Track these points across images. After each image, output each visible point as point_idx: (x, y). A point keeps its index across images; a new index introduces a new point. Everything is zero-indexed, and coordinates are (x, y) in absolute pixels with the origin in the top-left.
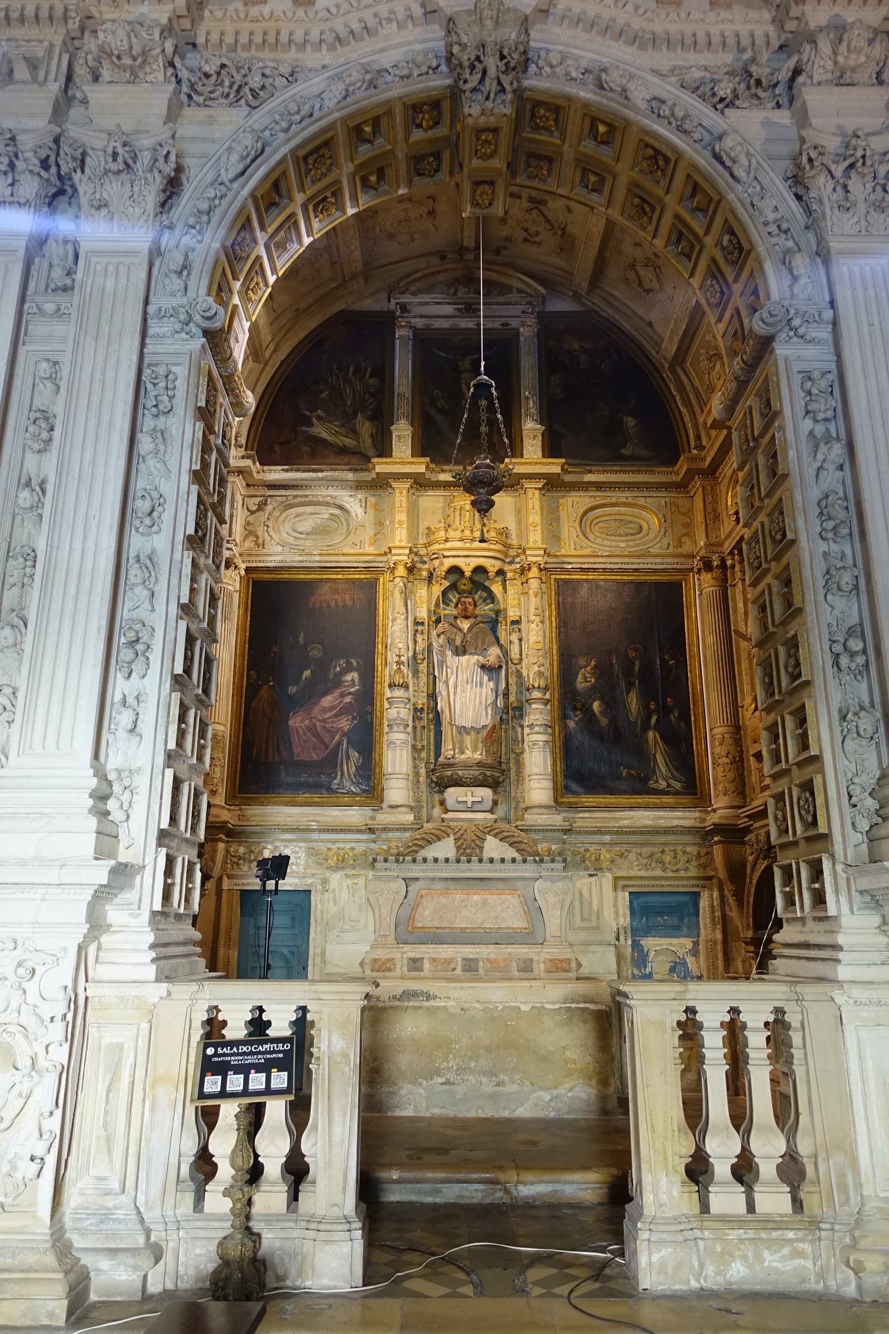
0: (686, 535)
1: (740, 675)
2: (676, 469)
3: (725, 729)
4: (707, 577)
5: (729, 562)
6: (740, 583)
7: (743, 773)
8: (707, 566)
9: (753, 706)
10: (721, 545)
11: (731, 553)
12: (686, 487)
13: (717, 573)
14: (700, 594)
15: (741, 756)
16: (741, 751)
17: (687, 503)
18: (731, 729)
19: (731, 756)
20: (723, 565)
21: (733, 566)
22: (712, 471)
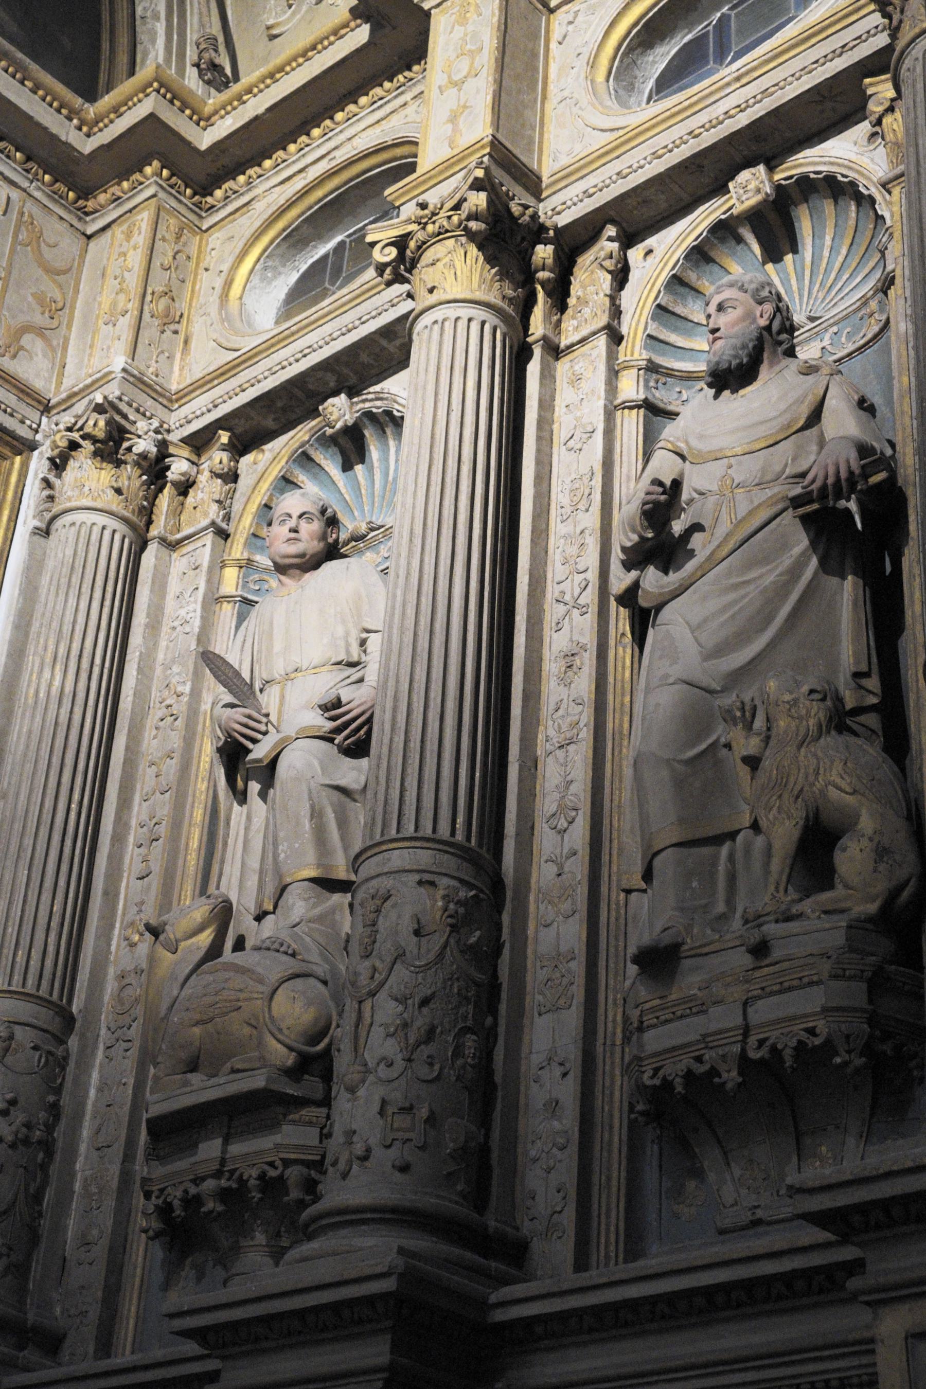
0: (40, 332)
1: (119, 839)
2: (91, 111)
3: (24, 1010)
4: (88, 478)
5: (178, 467)
6: (206, 546)
7: (38, 1198)
8: (111, 446)
9: (206, 938)
10: (171, 400)
11: (199, 442)
12: (85, 193)
13: (131, 478)
14: (45, 532)
15: (50, 1128)
16: (55, 1110)
17: (69, 244)
18: (44, 1016)
19: (19, 1117)
20: (155, 469)
21: (185, 487)
22: (206, 175)
